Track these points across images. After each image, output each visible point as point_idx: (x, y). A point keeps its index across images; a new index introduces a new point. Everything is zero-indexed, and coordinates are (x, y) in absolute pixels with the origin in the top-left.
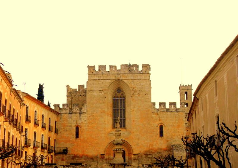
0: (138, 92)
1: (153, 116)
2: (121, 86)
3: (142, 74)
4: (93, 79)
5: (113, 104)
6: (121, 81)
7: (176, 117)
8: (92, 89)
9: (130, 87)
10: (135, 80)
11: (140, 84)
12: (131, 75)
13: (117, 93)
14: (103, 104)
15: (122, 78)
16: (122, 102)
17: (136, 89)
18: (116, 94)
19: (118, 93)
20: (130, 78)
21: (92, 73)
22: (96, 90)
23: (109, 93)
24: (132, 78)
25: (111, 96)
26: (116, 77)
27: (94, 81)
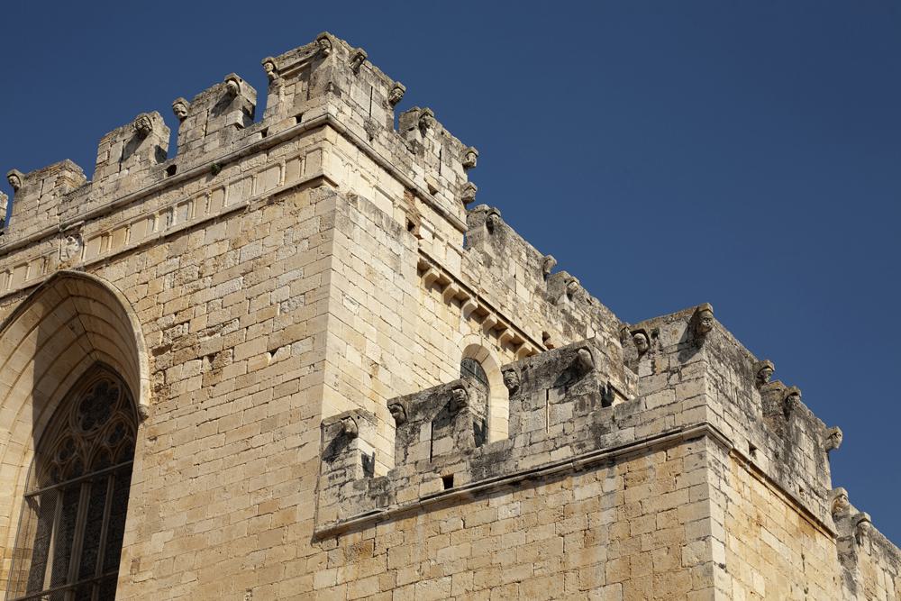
1: (324, 578)
7: (589, 537)
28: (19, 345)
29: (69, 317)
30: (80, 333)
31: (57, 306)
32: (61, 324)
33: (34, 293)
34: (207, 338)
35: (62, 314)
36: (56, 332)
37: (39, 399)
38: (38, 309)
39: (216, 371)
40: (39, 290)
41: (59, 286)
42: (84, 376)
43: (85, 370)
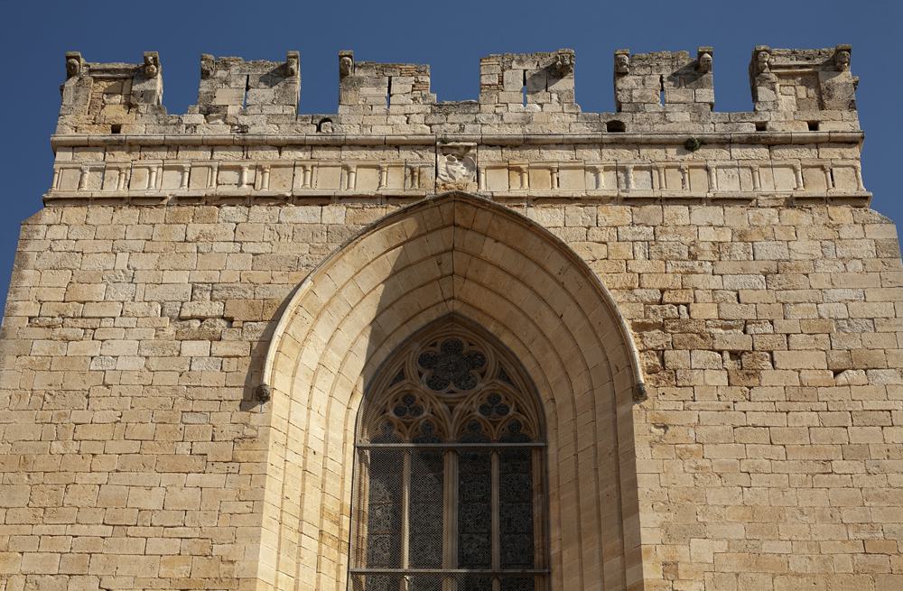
0: (736, 340)
2: (484, 300)
3: (771, 144)
4: (115, 188)
5: (356, 514)
6: (484, 219)
8: (84, 292)
9: (624, 279)
10: (670, 210)
11: (738, 248)
12: (625, 156)
13: (424, 387)
14: (214, 479)
15: (495, 185)
16: (486, 499)
17: (705, 310)
18: (409, 398)
19: (434, 384)
20: (607, 185)
21: (116, 129)
22: (139, 308)
23: (310, 357)
24: (639, 185)
25: (339, 412)
26: (413, 174)
27: (129, 214)
28: (373, 260)
29: (442, 248)
30: (446, 272)
31: (433, 230)
32: (430, 254)
33: (410, 206)
34: (721, 331)
35: (436, 242)
36: (419, 262)
37: (377, 334)
38: (410, 225)
39: (754, 373)
40: (421, 205)
41: (446, 208)
42: (431, 326)
43: (434, 317)
